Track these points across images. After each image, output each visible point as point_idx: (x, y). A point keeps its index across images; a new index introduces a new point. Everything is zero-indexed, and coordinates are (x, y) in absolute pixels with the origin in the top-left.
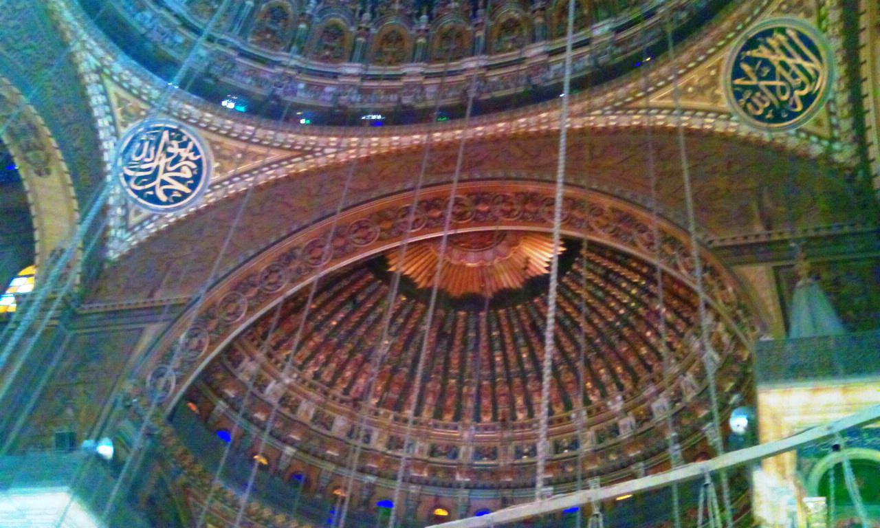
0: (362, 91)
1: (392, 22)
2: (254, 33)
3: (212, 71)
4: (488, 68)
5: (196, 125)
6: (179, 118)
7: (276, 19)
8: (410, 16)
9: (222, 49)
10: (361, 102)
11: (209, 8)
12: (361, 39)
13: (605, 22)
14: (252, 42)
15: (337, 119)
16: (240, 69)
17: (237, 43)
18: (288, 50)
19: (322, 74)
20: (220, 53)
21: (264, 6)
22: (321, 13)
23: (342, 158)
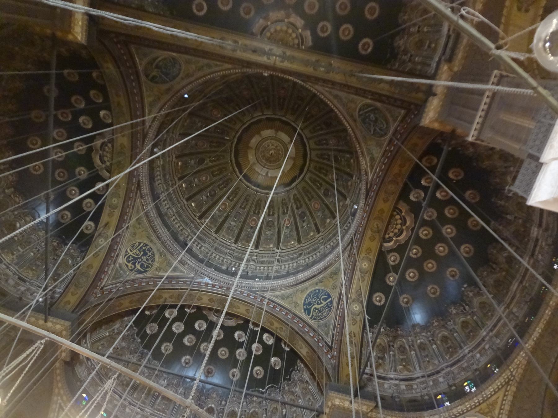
0: (497, 336)
1: (476, 301)
2: (446, 354)
3: (450, 384)
4: (521, 282)
5: (468, 411)
6: (461, 415)
7: (446, 342)
8: (478, 292)
9: (444, 372)
10: (501, 340)
11: (426, 362)
12: (475, 318)
13: (533, 228)
14: (449, 358)
15: (503, 357)
16: (456, 371)
17: (446, 364)
18: (461, 348)
19: (479, 344)
20: (445, 374)
21: (438, 342)
22: (455, 323)
23: (520, 371)
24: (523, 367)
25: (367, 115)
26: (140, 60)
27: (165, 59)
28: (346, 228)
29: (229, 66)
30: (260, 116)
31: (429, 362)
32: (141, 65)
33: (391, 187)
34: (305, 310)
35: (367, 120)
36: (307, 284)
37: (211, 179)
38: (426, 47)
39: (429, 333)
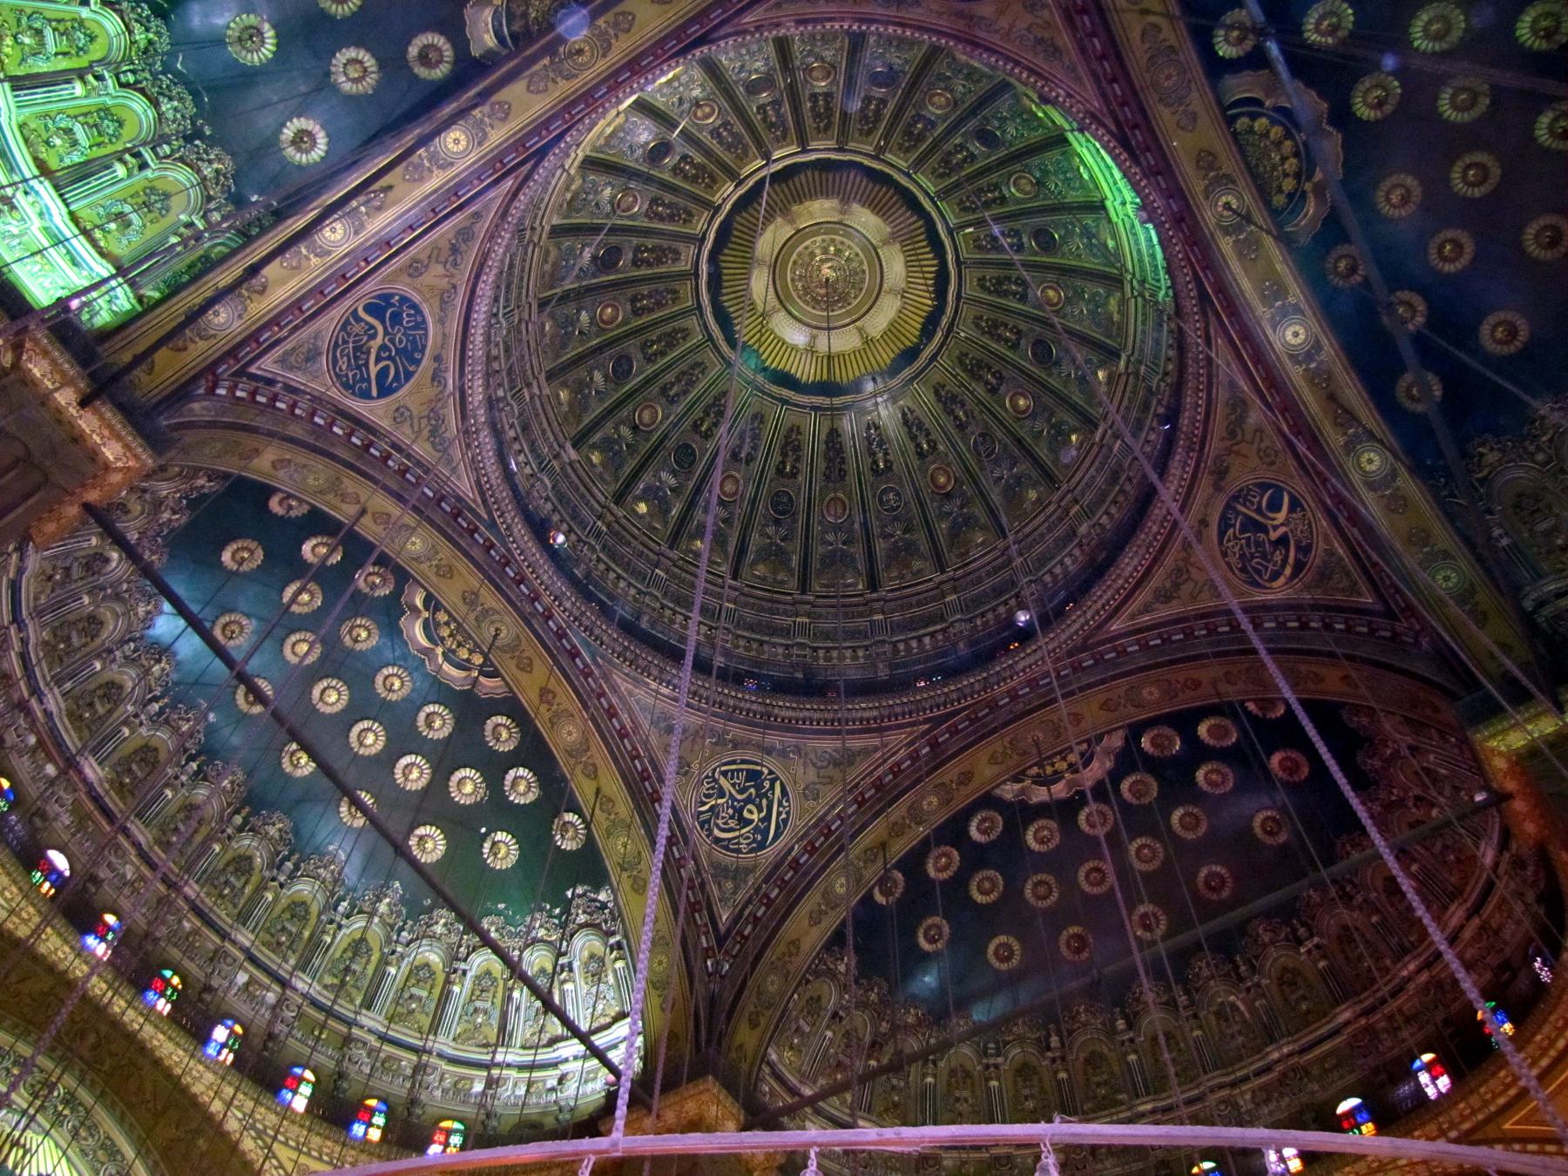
24: (10, 925)
25: (764, 802)
26: (1331, 553)
27: (1276, 575)
28: (496, 366)
29: (1116, 626)
30: (927, 194)
31: (50, 578)
32: (1326, 536)
33: (570, 733)
34: (387, 298)
35: (752, 790)
36: (454, 326)
37: (921, 105)
38: (802, 1022)
39: (125, 586)
